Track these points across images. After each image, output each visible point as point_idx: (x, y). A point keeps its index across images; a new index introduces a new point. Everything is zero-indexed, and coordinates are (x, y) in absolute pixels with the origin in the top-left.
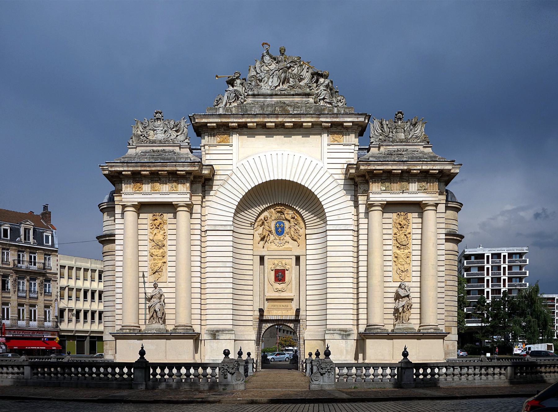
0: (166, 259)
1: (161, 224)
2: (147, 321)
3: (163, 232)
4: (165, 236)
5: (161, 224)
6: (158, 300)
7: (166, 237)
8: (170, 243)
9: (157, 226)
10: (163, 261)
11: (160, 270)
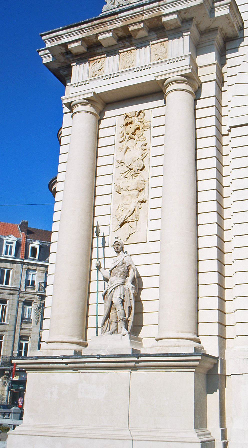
0: (146, 195)
1: (138, 129)
2: (100, 330)
3: (143, 143)
4: (145, 150)
5: (138, 129)
6: (120, 280)
7: (147, 152)
8: (155, 161)
9: (130, 134)
10: (140, 199)
11: (133, 217)
